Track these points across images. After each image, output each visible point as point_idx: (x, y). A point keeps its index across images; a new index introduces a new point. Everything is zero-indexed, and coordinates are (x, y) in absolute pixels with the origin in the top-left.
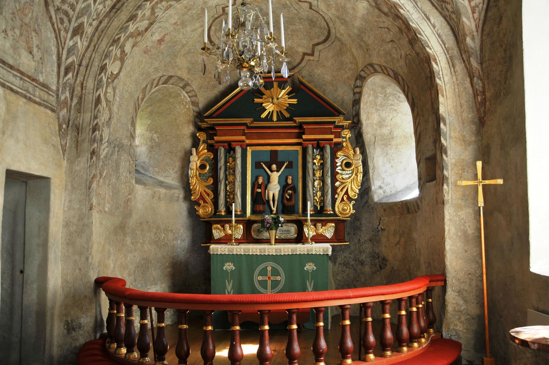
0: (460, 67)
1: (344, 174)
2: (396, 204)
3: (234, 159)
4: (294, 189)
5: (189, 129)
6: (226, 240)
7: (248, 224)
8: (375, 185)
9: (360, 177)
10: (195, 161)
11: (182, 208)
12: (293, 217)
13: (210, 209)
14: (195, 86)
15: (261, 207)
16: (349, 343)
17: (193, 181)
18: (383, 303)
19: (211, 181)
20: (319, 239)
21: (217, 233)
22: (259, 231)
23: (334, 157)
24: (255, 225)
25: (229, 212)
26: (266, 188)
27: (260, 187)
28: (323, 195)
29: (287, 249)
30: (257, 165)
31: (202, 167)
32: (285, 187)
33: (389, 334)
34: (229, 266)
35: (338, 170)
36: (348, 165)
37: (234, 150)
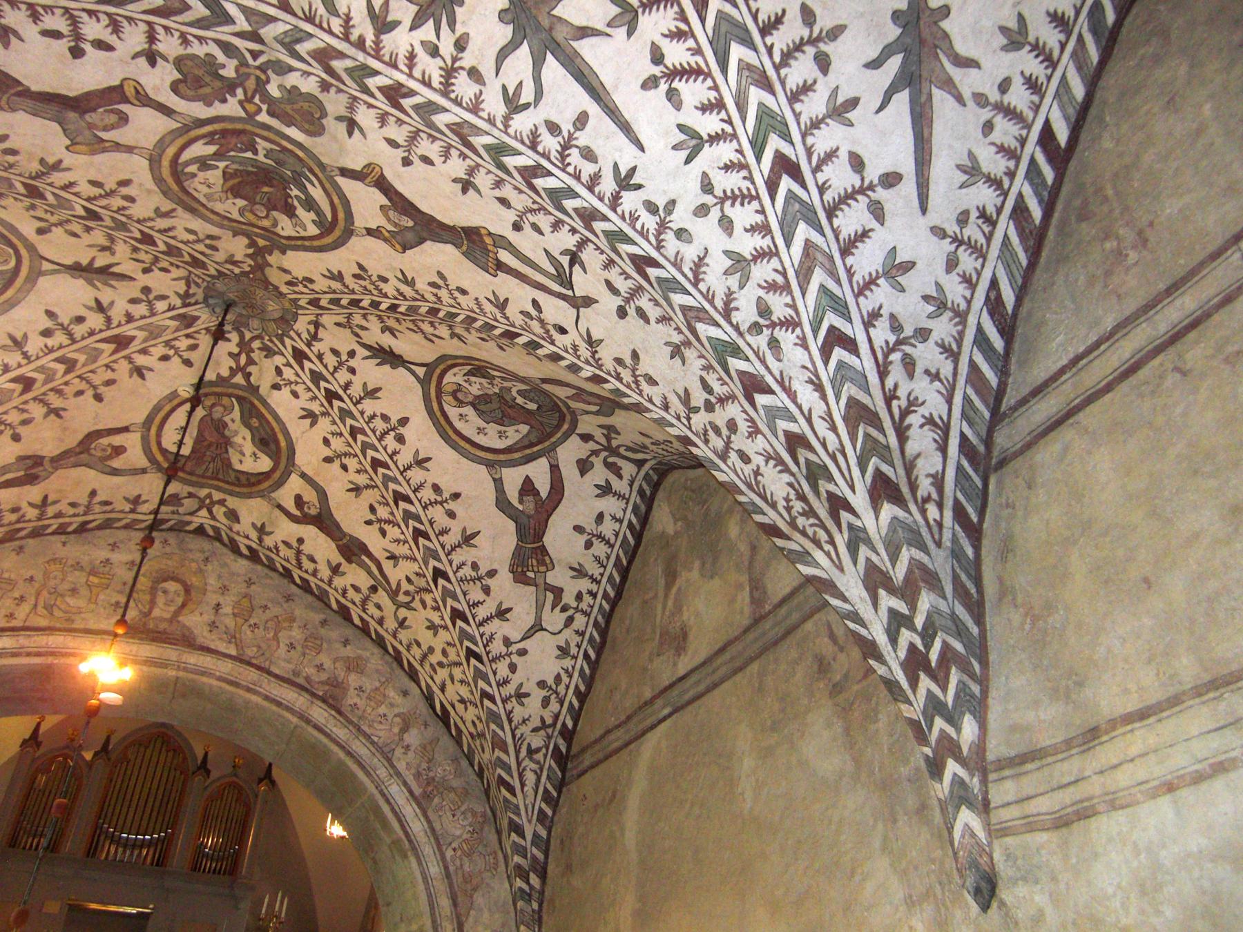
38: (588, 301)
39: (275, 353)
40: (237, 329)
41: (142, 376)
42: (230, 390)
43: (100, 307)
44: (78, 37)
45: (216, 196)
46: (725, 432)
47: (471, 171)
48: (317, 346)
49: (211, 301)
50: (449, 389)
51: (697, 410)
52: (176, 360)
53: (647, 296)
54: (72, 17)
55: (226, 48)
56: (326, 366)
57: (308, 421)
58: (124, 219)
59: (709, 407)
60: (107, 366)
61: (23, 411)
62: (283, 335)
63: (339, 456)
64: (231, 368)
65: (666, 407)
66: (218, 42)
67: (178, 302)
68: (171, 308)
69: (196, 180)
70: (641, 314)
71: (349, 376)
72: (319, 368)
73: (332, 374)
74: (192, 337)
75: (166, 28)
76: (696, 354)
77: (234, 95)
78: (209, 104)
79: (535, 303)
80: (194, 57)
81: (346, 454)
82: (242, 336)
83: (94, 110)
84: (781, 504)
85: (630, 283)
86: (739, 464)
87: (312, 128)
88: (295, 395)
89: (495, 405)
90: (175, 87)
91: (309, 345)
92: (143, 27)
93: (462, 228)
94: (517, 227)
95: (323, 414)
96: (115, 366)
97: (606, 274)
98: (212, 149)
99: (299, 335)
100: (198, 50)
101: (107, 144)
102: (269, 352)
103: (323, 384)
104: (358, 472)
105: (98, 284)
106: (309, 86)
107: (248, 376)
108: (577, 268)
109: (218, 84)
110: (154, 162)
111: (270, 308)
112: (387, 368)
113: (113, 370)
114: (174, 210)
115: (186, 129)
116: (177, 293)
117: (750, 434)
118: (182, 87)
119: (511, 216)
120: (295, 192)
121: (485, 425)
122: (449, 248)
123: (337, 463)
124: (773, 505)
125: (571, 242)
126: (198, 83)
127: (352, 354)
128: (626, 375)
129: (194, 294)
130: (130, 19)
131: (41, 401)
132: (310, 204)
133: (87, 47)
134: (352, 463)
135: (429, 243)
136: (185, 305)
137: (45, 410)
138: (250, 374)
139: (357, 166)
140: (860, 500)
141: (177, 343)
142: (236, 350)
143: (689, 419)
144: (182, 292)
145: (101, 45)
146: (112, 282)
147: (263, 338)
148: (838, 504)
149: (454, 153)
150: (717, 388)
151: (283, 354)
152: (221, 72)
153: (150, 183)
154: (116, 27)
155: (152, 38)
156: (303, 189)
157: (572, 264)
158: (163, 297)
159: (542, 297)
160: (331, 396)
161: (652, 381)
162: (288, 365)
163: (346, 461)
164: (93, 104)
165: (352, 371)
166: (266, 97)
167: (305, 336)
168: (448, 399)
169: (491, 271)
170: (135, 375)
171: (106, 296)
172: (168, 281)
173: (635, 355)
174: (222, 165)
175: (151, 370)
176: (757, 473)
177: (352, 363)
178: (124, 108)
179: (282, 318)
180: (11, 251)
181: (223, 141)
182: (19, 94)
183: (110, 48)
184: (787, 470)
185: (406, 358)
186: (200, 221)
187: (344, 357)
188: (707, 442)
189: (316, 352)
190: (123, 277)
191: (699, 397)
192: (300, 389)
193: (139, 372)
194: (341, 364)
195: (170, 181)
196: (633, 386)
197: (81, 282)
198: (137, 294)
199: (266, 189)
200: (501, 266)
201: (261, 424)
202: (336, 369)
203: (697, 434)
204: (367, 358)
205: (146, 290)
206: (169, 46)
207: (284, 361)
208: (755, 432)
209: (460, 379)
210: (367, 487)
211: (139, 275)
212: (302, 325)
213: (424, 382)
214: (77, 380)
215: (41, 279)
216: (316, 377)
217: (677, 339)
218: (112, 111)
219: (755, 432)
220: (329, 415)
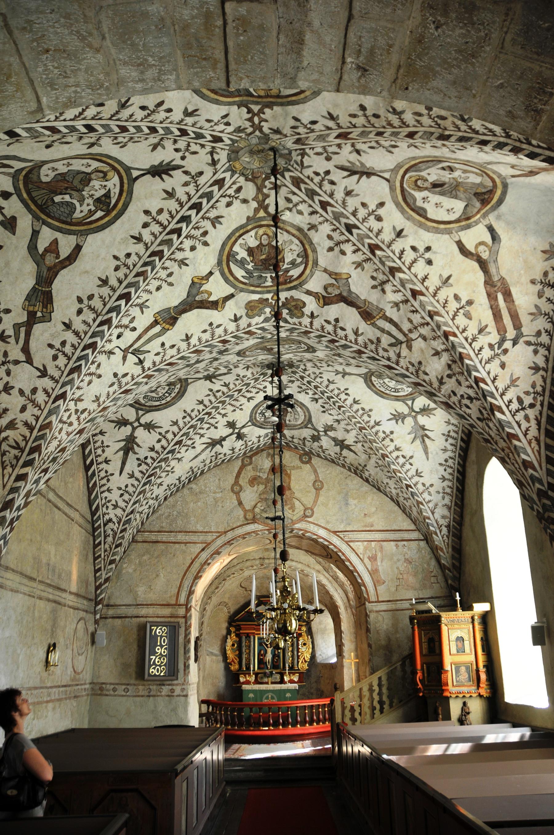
0: (349, 610)
1: (302, 649)
2: (327, 664)
3: (250, 642)
4: (279, 657)
5: (225, 625)
6: (248, 683)
7: (256, 674)
8: (318, 654)
9: (311, 650)
10: (229, 642)
11: (222, 665)
12: (278, 671)
13: (237, 667)
14: (230, 605)
15: (262, 666)
16: (307, 719)
17: (229, 652)
18: (319, 705)
19: (237, 652)
20: (292, 682)
21: (242, 679)
22: (262, 678)
23: (298, 640)
24: (260, 675)
25: (248, 668)
26: (265, 656)
27: (262, 655)
28: (293, 659)
29: (278, 687)
30: (260, 644)
31: (233, 645)
32: (274, 656)
33: (321, 717)
34: (251, 695)
35: (300, 647)
36: (305, 644)
37: (250, 637)
38: (124, 358)
39: (234, 131)
40: (266, 135)
41: (329, 114)
42: (260, 100)
43: (358, 152)
44: (335, 326)
45: (287, 244)
46: (69, 421)
47: (189, 344)
48: (208, 149)
49: (286, 152)
50: (111, 174)
51: (76, 405)
52: (305, 121)
53: (117, 389)
54: (335, 333)
55: (286, 321)
56: (196, 143)
57: (190, 110)
58: (335, 222)
59: (77, 411)
60: (355, 126)
61: (418, 121)
62: (233, 144)
63: (154, 111)
64: (264, 113)
65: (78, 388)
66: (290, 323)
67: (307, 151)
68: (313, 148)
69: (297, 253)
70: (112, 385)
71: (177, 146)
72: (201, 141)
73: (189, 143)
74: (296, 133)
75: (306, 327)
76: (95, 408)
77: (282, 302)
78: (292, 297)
79: (134, 329)
80: (298, 317)
81: (149, 115)
82: (261, 131)
83: (336, 295)
84: (46, 451)
85: (124, 384)
86: (58, 429)
87: (250, 305)
88: (208, 121)
89: (76, 183)
90: (304, 304)
91: (213, 148)
92: (314, 327)
93: (177, 319)
94: (163, 344)
95: (182, 120)
96: (349, 125)
97: (130, 375)
98: (290, 273)
99: (222, 149)
100: (295, 320)
101: (334, 277)
102: (239, 130)
103: (193, 135)
104: (132, 116)
105: (358, 163)
106: (254, 321)
107: (249, 111)
108: (137, 360)
109: (289, 306)
110: (316, 263)
111: (247, 155)
112: (156, 163)
113: (351, 123)
114: (309, 230)
115: (301, 285)
116: (309, 156)
117: (67, 432)
118: (302, 305)
119: (167, 346)
120: (250, 267)
121: (70, 168)
122: (176, 303)
123: (152, 107)
124: (46, 449)
125: (147, 364)
126: (296, 307)
127: (183, 158)
128: (93, 368)
129: (298, 155)
130: (318, 330)
131: (404, 123)
132: (242, 263)
133: (333, 323)
134: (140, 114)
135: (185, 297)
136: (304, 149)
137: (403, 116)
138: (248, 112)
139: (228, 303)
140: (48, 476)
141: (305, 130)
142: (263, 124)
143: (73, 400)
144: (306, 157)
145: (328, 322)
146: (348, 164)
147: (246, 135)
148: (46, 471)
149: (198, 343)
150: (83, 416)
151: (229, 134)
152: (287, 311)
153: (319, 249)
154: (323, 327)
155: (311, 323)
156: (247, 271)
157: (139, 359)
158: (318, 154)
159: (136, 334)
160: (184, 133)
161: (90, 383)
162: (222, 132)
163: (146, 112)
164: (336, 298)
165: (177, 150)
166: (270, 305)
167: (218, 150)
168: (106, 168)
169: (157, 315)
170: (335, 116)
171: (354, 157)
172: (315, 165)
173: (100, 376)
174: (285, 266)
175: (323, 117)
176: (56, 438)
177: (180, 154)
178: (325, 294)
179: (238, 152)
180: (405, 186)
181: (286, 278)
182: (361, 308)
183: (326, 321)
184: (56, 449)
185: (148, 177)
186: (295, 223)
187: (187, 154)
188: (65, 411)
189: (206, 147)
190: (342, 168)
191: (81, 406)
192: (207, 125)
193: (332, 117)
194: (187, 150)
195: (309, 251)
196: (89, 371)
197: (368, 165)
198: (334, 157)
199: (264, 257)
200: (156, 323)
201: (228, 91)
202: (189, 145)
203: (67, 405)
204: (172, 161)
205: (328, 159)
206: (306, 321)
207: (226, 131)
208: (68, 434)
209: (109, 184)
210: (117, 113)
211: (332, 169)
212: (222, 156)
213: (128, 169)
214: (376, 125)
215: (392, 167)
216: (199, 136)
217: (101, 400)
218: (329, 294)
219: (68, 434)
220: (178, 124)
